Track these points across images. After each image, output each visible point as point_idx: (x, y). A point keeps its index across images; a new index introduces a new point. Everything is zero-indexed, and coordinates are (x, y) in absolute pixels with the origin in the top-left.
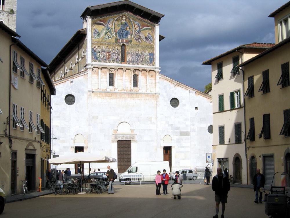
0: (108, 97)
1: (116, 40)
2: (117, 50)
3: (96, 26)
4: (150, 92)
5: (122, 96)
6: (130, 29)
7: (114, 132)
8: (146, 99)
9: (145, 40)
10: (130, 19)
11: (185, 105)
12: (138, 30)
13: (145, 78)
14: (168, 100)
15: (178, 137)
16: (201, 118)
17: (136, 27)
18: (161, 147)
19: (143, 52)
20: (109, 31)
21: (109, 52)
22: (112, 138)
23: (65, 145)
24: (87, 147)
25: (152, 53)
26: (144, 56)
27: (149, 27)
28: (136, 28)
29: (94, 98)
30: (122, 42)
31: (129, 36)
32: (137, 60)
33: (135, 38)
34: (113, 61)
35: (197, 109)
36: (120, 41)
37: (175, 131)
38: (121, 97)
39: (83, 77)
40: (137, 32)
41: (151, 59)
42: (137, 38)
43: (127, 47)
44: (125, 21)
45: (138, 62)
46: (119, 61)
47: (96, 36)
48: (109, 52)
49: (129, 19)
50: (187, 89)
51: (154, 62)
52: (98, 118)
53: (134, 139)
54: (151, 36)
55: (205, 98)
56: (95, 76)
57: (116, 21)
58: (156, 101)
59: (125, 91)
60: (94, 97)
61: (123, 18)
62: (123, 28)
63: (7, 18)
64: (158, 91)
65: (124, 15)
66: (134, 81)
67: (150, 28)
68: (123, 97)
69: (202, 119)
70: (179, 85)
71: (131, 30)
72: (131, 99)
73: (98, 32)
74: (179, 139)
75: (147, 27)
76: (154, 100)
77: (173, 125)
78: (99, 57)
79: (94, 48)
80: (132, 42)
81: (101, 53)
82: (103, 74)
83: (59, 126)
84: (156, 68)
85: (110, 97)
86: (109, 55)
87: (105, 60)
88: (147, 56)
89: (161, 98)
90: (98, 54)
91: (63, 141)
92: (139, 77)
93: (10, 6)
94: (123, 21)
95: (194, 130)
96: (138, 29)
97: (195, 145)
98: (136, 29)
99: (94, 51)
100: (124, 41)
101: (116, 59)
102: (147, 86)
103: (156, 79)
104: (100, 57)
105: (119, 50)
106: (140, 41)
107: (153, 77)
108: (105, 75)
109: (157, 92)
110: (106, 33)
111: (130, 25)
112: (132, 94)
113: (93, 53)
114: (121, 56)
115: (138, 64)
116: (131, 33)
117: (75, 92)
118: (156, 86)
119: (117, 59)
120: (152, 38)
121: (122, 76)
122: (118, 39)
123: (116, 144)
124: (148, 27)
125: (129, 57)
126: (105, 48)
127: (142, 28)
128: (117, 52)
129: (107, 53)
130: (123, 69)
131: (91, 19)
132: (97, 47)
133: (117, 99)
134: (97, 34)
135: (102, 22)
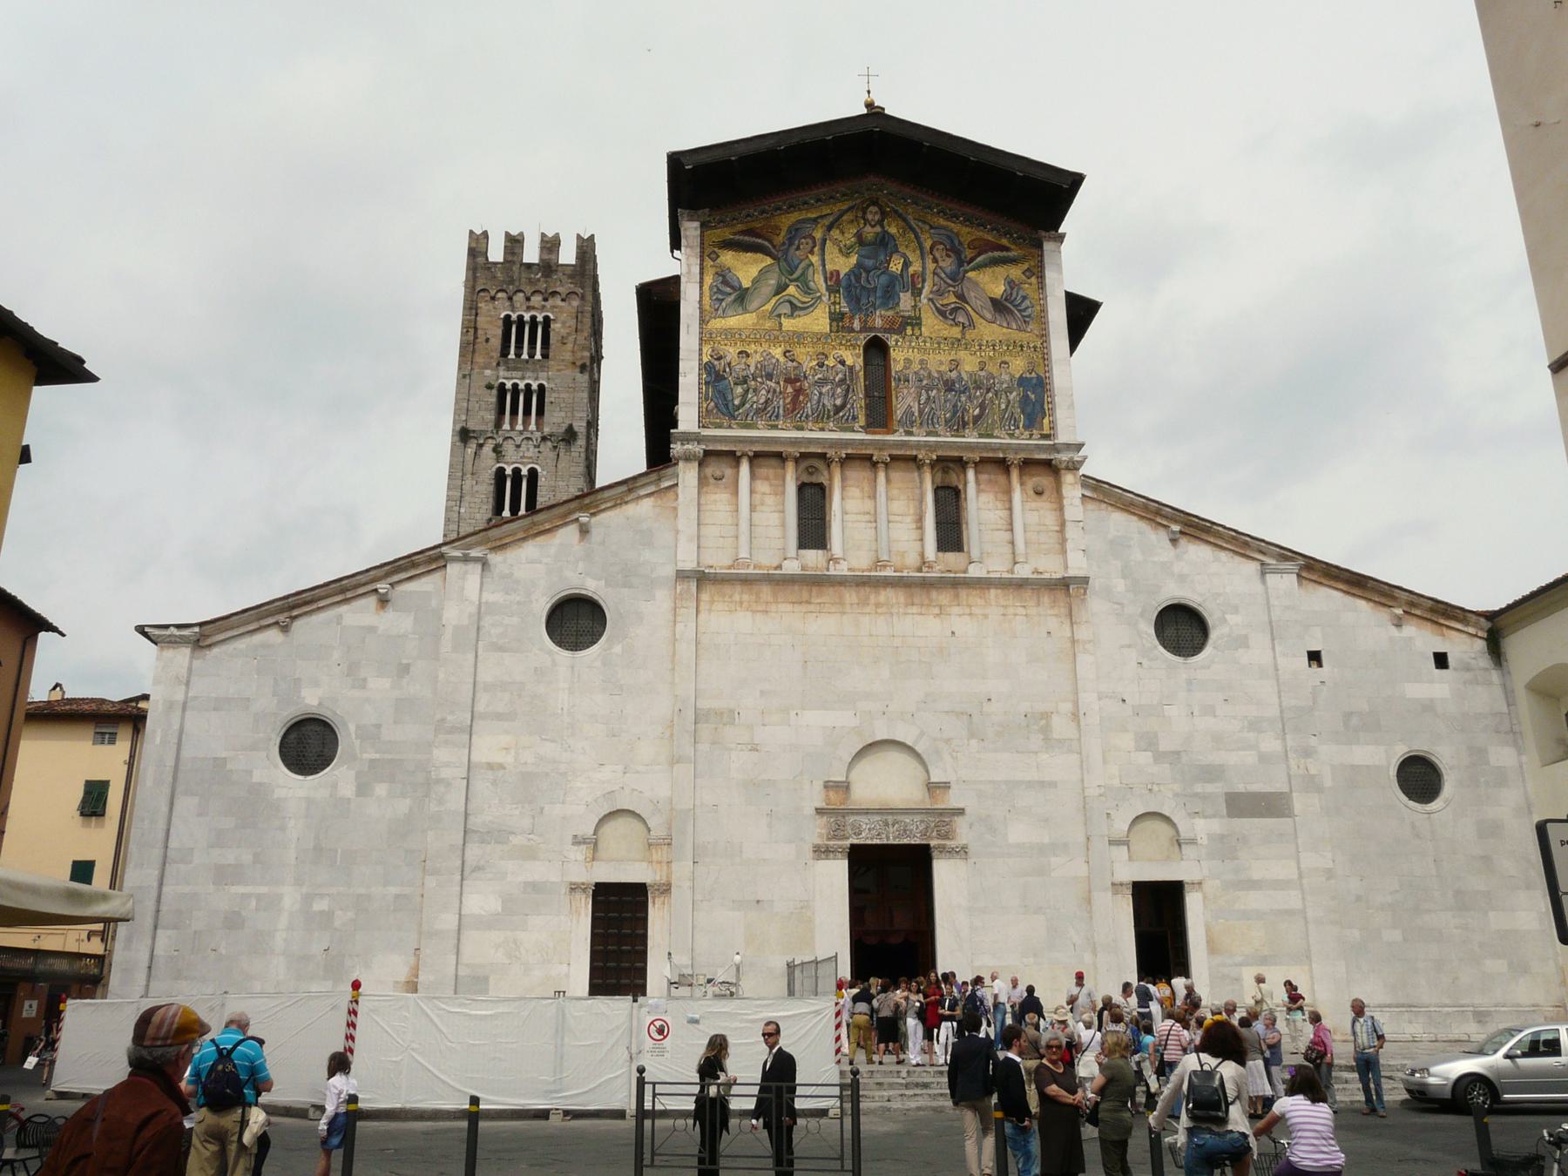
0: (789, 607)
1: (832, 320)
2: (839, 366)
3: (728, 258)
4: (1035, 576)
5: (873, 599)
6: (906, 264)
7: (827, 796)
8: (1011, 610)
9: (989, 316)
10: (905, 220)
11: (1243, 642)
12: (948, 270)
13: (999, 505)
14: (1142, 615)
15: (1216, 826)
16: (1348, 715)
17: (937, 255)
18: (1113, 884)
19: (983, 373)
20: (796, 280)
21: (798, 380)
22: (816, 832)
23: (538, 871)
24: (666, 889)
25: (1033, 375)
26: (990, 395)
27: (1007, 249)
28: (940, 259)
29: (710, 610)
30: (864, 329)
31: (906, 301)
32: (955, 413)
33: (937, 308)
34: (821, 417)
35: (1320, 665)
36: (857, 325)
37: (1199, 788)
38: (864, 602)
39: (648, 503)
40: (943, 275)
41: (1029, 409)
42: (947, 305)
43: (893, 354)
44: (878, 229)
45: (959, 423)
46: (854, 418)
47: (724, 304)
48: (796, 380)
49: (900, 216)
50: (1249, 553)
51: (1046, 421)
52: (732, 722)
53: (946, 837)
54: (1021, 293)
55: (1362, 603)
56: (717, 497)
57: (830, 228)
58: (1072, 624)
59: (889, 573)
60: (712, 602)
61: (870, 217)
62: (869, 263)
63: (553, 455)
64: (1077, 565)
65: (875, 203)
66: (940, 524)
67: (1011, 254)
68: (878, 605)
69: (1355, 721)
70: (1198, 533)
71: (911, 270)
72: (921, 614)
73: (736, 284)
74: (1222, 837)
75: (997, 254)
76: (1056, 615)
77: (1178, 753)
78: (743, 404)
79: (716, 363)
80: (919, 325)
81: (753, 383)
82: (763, 487)
83: (504, 768)
84: (1055, 448)
85: (801, 603)
86: (798, 392)
87: (777, 417)
88: (1009, 390)
89: (1095, 605)
90: (739, 390)
91: (529, 854)
92: (966, 499)
93: (563, 414)
94: (868, 229)
95: (1312, 784)
96: (948, 264)
97: (1330, 874)
98: (941, 264)
99: (713, 376)
100: (878, 323)
101: (836, 413)
102: (1012, 543)
103: (1065, 502)
104: (747, 406)
105: (851, 368)
106: (961, 319)
107: (1045, 497)
108: (776, 494)
109: (1071, 573)
110: (781, 289)
111: (907, 247)
112: (927, 585)
113: (707, 383)
114: (861, 396)
115: (957, 433)
116: (913, 282)
117: (603, 582)
118: (1063, 541)
119: (838, 409)
120: (1027, 303)
121: (873, 497)
122: (843, 315)
123: (839, 870)
124: (1005, 254)
125: (904, 401)
126: (774, 361)
127: (972, 260)
128: (840, 376)
129: (788, 381)
130: (874, 458)
131: (696, 224)
132: (728, 359)
133: (844, 613)
134: (733, 297)
135: (759, 236)
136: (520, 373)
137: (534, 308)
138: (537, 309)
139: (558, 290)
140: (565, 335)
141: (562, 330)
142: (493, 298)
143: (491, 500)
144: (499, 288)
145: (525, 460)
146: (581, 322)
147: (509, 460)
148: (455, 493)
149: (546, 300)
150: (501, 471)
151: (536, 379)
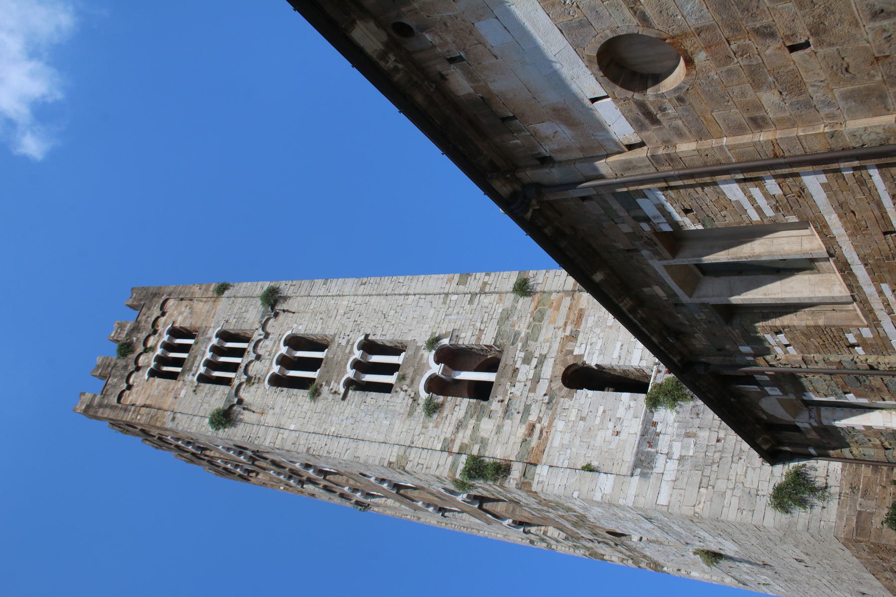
136: (199, 358)
137: (156, 345)
138: (158, 342)
139: (153, 319)
140: (189, 311)
141: (185, 314)
142: (129, 387)
143: (295, 391)
144: (125, 380)
145: (274, 351)
146: (186, 294)
147: (267, 368)
148: (271, 433)
149: (155, 332)
150: (277, 381)
151: (210, 339)
